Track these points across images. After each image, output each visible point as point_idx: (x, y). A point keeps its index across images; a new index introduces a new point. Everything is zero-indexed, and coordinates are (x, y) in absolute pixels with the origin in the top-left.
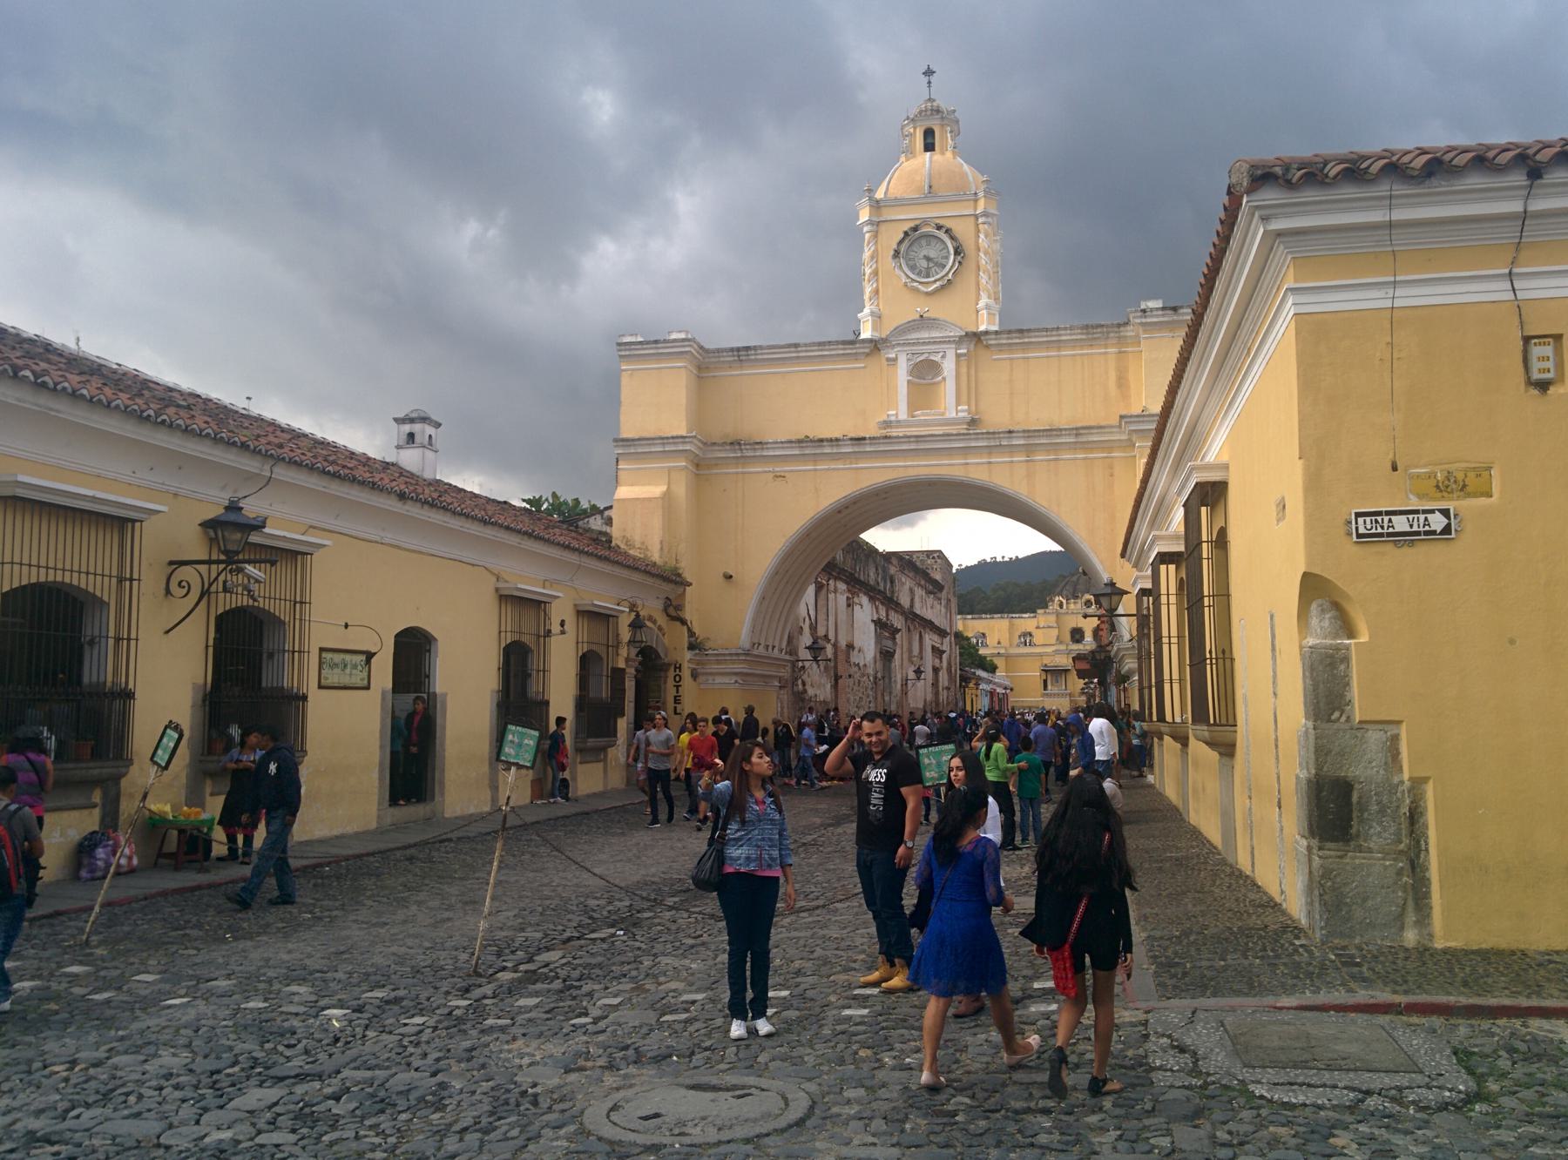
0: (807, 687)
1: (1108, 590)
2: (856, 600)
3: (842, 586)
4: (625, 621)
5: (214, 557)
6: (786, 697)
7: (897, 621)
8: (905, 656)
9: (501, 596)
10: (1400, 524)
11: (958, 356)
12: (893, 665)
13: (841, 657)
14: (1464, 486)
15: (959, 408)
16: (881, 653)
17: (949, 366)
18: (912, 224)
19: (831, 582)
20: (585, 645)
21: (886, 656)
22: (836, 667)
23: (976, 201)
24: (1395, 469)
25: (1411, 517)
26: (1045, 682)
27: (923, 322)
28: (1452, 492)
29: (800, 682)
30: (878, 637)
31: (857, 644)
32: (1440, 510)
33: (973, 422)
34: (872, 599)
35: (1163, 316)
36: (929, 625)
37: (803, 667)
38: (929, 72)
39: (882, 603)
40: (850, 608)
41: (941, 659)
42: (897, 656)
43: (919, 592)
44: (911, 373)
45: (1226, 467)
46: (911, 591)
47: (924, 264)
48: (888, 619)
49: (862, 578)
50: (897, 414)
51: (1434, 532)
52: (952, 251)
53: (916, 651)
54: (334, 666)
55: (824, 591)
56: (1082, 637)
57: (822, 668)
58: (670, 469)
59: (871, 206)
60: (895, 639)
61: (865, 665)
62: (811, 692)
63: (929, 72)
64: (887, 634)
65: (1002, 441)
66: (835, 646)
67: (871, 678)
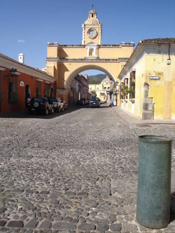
17: (95, 50)
18: (90, 28)
27: (92, 43)
33: (98, 58)
38: (93, 6)
63: (93, 6)
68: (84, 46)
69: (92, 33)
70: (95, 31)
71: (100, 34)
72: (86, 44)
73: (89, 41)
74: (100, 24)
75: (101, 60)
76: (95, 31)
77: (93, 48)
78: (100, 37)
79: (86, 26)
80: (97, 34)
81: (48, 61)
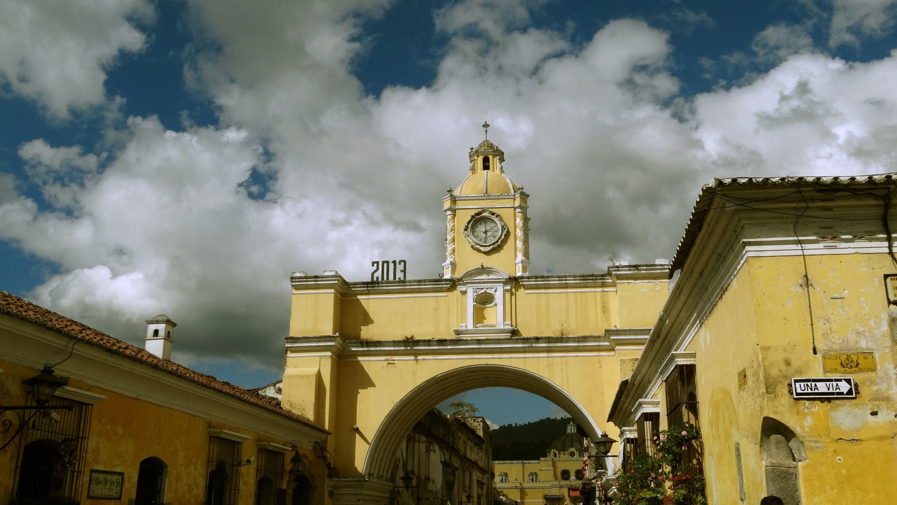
1: (604, 439)
3: (423, 438)
4: (289, 457)
5: (28, 405)
7: (456, 462)
8: (461, 486)
9: (210, 437)
10: (822, 387)
11: (506, 291)
14: (858, 364)
15: (505, 323)
16: (446, 484)
17: (499, 296)
18: (476, 211)
19: (417, 435)
20: (263, 473)
21: (449, 485)
23: (515, 199)
24: (815, 353)
25: (828, 383)
27: (483, 270)
28: (851, 367)
29: (396, 502)
30: (445, 473)
31: (432, 476)
32: (844, 379)
34: (441, 448)
35: (629, 270)
36: (475, 464)
37: (398, 492)
42: (456, 486)
43: (469, 444)
44: (475, 300)
45: (694, 355)
46: (465, 443)
47: (484, 236)
48: (450, 461)
50: (466, 325)
51: (842, 393)
52: (501, 228)
53: (467, 484)
54: (98, 482)
57: (410, 492)
58: (321, 356)
59: (451, 200)
60: (454, 474)
61: (436, 492)
65: (532, 344)
66: (418, 478)
67: (440, 501)
68: (453, 284)
69: (486, 232)
70: (496, 220)
71: (519, 233)
72: (457, 275)
73: (472, 260)
74: (518, 195)
75: (526, 340)
76: (496, 220)
77: (488, 291)
78: (520, 244)
79: (460, 205)
80: (508, 232)
81: (292, 352)
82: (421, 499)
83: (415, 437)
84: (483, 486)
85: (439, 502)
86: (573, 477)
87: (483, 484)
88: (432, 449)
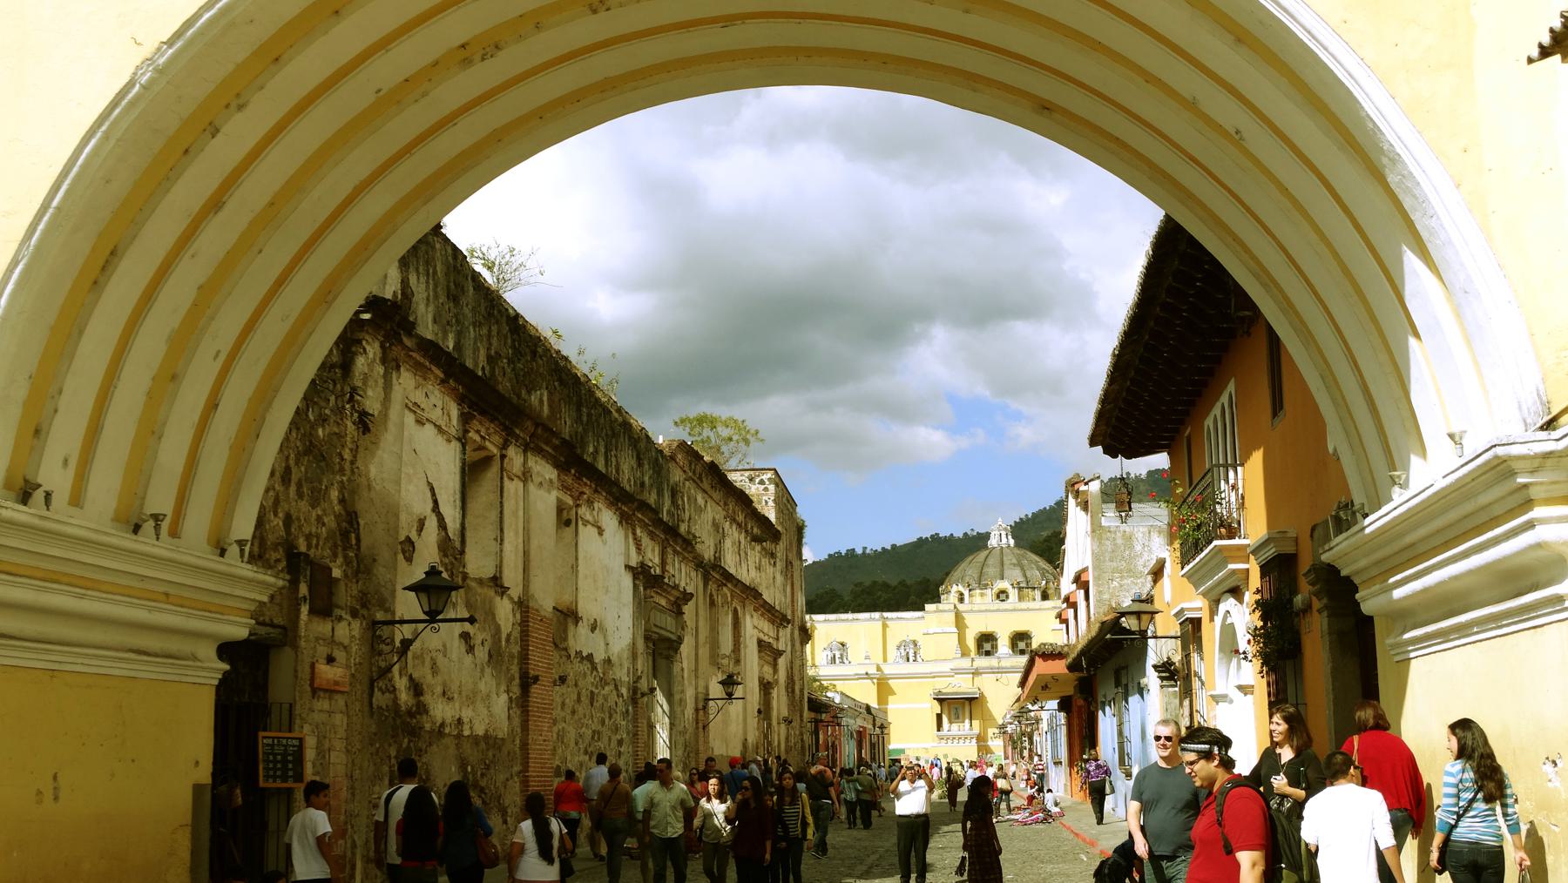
0: (427, 698)
2: (583, 511)
3: (544, 470)
6: (339, 720)
7: (684, 576)
8: (704, 652)
12: (676, 668)
13: (539, 634)
16: (647, 638)
19: (515, 456)
22: (524, 657)
26: (939, 717)
30: (642, 606)
31: (587, 608)
34: (625, 520)
36: (750, 593)
39: (652, 536)
40: (570, 531)
41: (775, 666)
42: (686, 649)
43: (733, 535)
46: (716, 526)
48: (664, 570)
49: (601, 466)
55: (492, 474)
56: (995, 647)
60: (680, 613)
61: (608, 661)
62: (441, 711)
64: (663, 602)
66: (523, 606)
67: (624, 691)
82: (536, 679)
83: (503, 457)
84: (775, 660)
85: (620, 695)
86: (1004, 646)
87: (779, 653)
88: (588, 517)
